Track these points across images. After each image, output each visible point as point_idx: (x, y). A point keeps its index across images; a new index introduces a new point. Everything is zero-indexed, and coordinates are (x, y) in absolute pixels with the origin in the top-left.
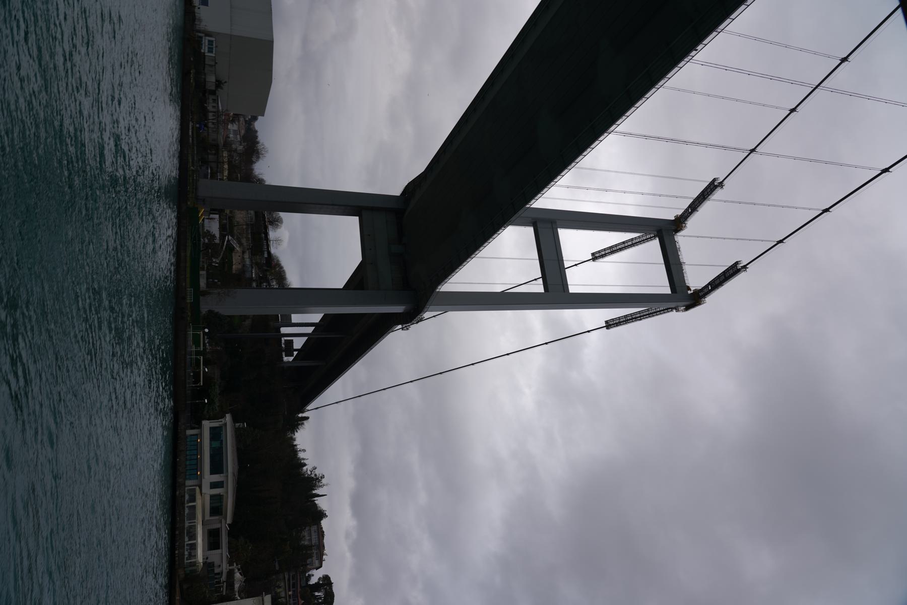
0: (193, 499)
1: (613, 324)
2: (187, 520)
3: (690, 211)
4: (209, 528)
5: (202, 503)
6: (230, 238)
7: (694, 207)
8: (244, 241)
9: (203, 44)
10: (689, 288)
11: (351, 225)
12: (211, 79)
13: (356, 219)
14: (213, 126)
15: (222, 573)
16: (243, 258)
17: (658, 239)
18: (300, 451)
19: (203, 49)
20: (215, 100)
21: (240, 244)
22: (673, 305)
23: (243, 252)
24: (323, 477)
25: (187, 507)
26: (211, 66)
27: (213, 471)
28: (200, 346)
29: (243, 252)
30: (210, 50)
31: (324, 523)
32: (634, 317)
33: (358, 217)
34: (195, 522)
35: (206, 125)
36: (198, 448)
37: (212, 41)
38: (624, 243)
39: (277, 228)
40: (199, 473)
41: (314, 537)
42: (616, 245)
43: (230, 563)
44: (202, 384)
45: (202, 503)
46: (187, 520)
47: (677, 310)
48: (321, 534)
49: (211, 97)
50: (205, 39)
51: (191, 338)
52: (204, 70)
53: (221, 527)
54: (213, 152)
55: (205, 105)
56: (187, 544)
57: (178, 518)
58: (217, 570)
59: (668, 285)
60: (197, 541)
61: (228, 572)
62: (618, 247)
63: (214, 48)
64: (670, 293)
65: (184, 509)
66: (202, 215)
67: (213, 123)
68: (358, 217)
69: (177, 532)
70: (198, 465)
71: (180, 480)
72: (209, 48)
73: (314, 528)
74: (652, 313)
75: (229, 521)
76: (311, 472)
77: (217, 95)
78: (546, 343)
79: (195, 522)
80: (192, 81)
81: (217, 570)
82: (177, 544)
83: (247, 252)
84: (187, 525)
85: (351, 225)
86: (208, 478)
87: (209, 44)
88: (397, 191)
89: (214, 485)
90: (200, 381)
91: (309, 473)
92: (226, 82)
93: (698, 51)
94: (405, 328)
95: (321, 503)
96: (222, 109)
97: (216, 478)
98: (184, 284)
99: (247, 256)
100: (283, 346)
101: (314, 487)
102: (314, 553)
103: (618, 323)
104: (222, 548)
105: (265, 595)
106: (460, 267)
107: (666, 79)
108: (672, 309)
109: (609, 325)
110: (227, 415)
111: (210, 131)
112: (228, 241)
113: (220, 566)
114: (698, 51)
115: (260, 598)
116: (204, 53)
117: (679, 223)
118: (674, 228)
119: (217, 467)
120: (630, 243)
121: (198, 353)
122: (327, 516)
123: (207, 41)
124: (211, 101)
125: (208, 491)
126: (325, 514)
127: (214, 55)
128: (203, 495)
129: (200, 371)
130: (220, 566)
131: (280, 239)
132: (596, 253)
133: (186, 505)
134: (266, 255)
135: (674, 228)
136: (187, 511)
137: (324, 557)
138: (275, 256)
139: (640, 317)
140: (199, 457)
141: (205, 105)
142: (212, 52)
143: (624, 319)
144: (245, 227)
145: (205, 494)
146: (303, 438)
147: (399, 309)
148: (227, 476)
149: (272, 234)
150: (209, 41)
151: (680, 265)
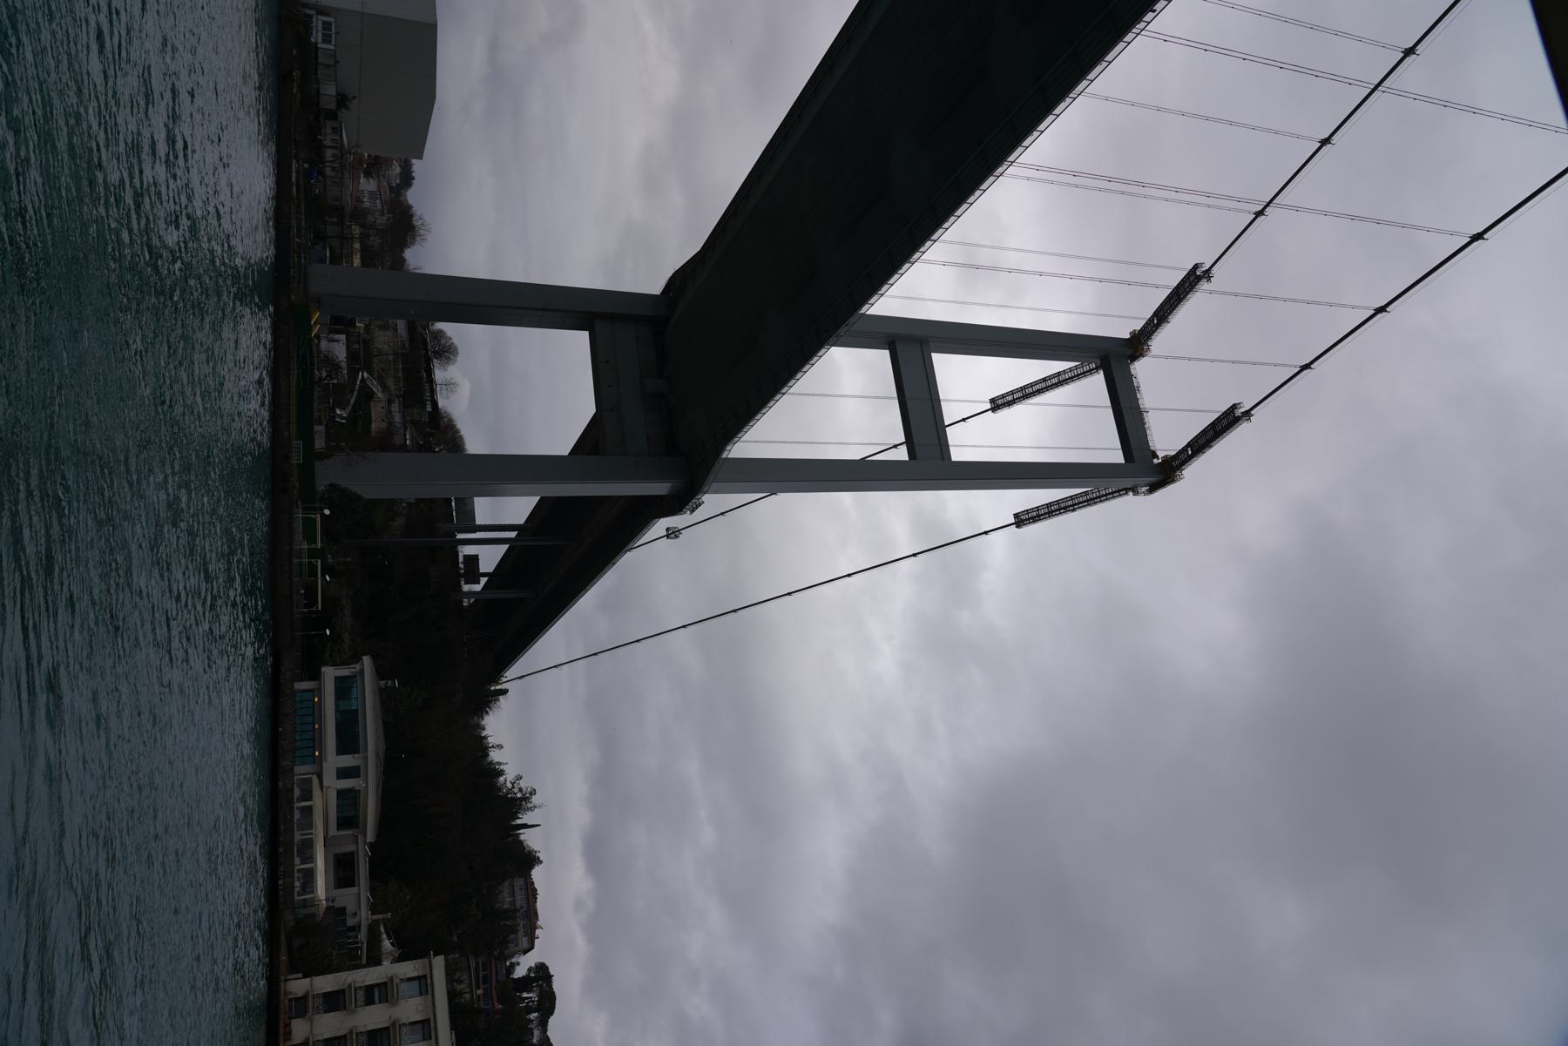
0: (307, 796)
1: (1026, 520)
2: (298, 830)
3: (1156, 322)
4: (336, 852)
5: (323, 804)
6: (365, 375)
7: (1162, 315)
8: (390, 382)
9: (314, 28)
10: (1155, 455)
11: (578, 343)
12: (329, 90)
13: (584, 336)
14: (333, 174)
15: (360, 926)
16: (390, 412)
17: (1102, 372)
18: (493, 747)
19: (314, 35)
20: (336, 129)
21: (385, 388)
22: (1129, 483)
23: (390, 402)
24: (533, 792)
25: (298, 808)
26: (328, 66)
27: (341, 751)
28: (316, 543)
29: (390, 402)
30: (326, 39)
31: (537, 874)
32: (1062, 505)
33: (587, 333)
34: (311, 834)
35: (321, 173)
36: (316, 712)
37: (329, 24)
38: (1044, 380)
39: (447, 363)
40: (317, 753)
41: (520, 899)
42: (1032, 385)
43: (374, 909)
44: (320, 608)
45: (323, 804)
46: (298, 830)
47: (1134, 490)
48: (531, 893)
49: (329, 124)
50: (317, 19)
51: (299, 526)
52: (316, 74)
53: (358, 850)
54: (335, 220)
55: (319, 137)
56: (299, 871)
57: (282, 827)
58: (350, 922)
59: (1120, 447)
60: (316, 865)
61: (369, 925)
62: (1035, 388)
63: (333, 36)
64: (1123, 462)
65: (292, 810)
66: (316, 323)
67: (333, 168)
68: (587, 333)
69: (281, 850)
70: (316, 741)
72: (324, 35)
73: (519, 882)
74: (1094, 499)
75: (370, 837)
76: (513, 784)
77: (340, 120)
78: (914, 555)
79: (311, 834)
80: (295, 90)
81: (350, 922)
83: (397, 401)
84: (297, 837)
85: (578, 343)
86: (333, 761)
87: (324, 29)
88: (655, 287)
89: (343, 773)
90: (317, 603)
91: (509, 785)
92: (354, 97)
93: (1156, 13)
94: (673, 535)
95: (530, 838)
96: (349, 143)
98: (286, 433)
99: (395, 407)
100: (462, 566)
102: (518, 925)
103: (1035, 517)
104: (359, 886)
105: (434, 956)
106: (764, 411)
107: (1105, 64)
108: (1127, 490)
109: (1021, 520)
110: (364, 657)
112: (363, 380)
113: (355, 914)
114: (1156, 13)
115: (426, 960)
116: (316, 43)
117: (1137, 345)
118: (1129, 352)
119: (348, 741)
120: (1055, 380)
121: (313, 553)
122: (541, 862)
123: (320, 23)
124: (329, 131)
125: (333, 784)
126: (538, 857)
127: (333, 47)
128: (324, 789)
129: (317, 581)
130: (355, 914)
131: (453, 381)
132: (998, 397)
133: (295, 806)
134: (429, 409)
135: (1129, 352)
136: (297, 815)
137: (538, 932)
138: (445, 412)
139: (1073, 505)
140: (317, 726)
141: (319, 137)
142: (330, 42)
143: (1046, 510)
144: (391, 358)
145: (327, 788)
146: (498, 726)
147: (660, 488)
148: (366, 758)
149: (439, 375)
150: (324, 23)
151: (1138, 414)
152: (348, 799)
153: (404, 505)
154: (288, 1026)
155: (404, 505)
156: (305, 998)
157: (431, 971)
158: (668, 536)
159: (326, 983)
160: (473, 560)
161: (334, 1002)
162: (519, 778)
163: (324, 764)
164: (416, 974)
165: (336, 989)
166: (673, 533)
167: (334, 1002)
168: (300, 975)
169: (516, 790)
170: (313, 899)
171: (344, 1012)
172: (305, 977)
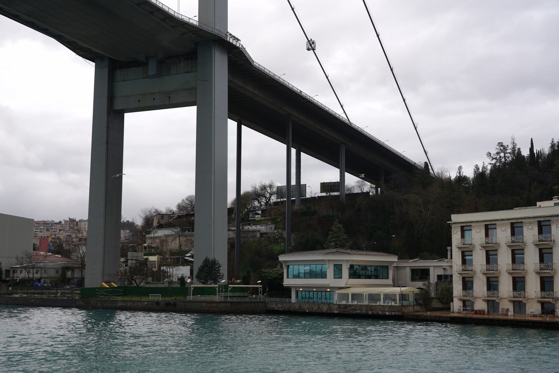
2: (363, 303)
13: (129, 117)
14: (39, 273)
18: (460, 173)
24: (500, 144)
25: (352, 302)
34: (366, 294)
35: (39, 280)
36: (308, 289)
40: (328, 290)
51: (199, 297)
53: (410, 267)
55: (18, 281)
56: (384, 302)
65: (352, 305)
69: (370, 313)
70: (322, 289)
71: (325, 309)
76: (493, 159)
79: (366, 294)
82: (380, 313)
84: (366, 303)
94: (313, 45)
97: (330, 272)
98: (146, 303)
100: (331, 194)
101: (518, 155)
104: (429, 266)
111: (46, 276)
113: (444, 269)
115: (453, 226)
125: (345, 280)
128: (347, 286)
130: (444, 269)
136: (355, 303)
141: (18, 281)
148: (329, 260)
152: (355, 273)
153: (276, 231)
154: (476, 312)
155: (276, 231)
156: (464, 302)
157: (459, 223)
158: (314, 50)
159: (457, 288)
160: (325, 187)
161: (467, 284)
162: (489, 154)
163: (330, 286)
164: (459, 233)
165: (461, 282)
166: (311, 45)
167: (467, 284)
168: (451, 303)
169: (498, 157)
170: (400, 295)
171: (475, 277)
172: (453, 301)
